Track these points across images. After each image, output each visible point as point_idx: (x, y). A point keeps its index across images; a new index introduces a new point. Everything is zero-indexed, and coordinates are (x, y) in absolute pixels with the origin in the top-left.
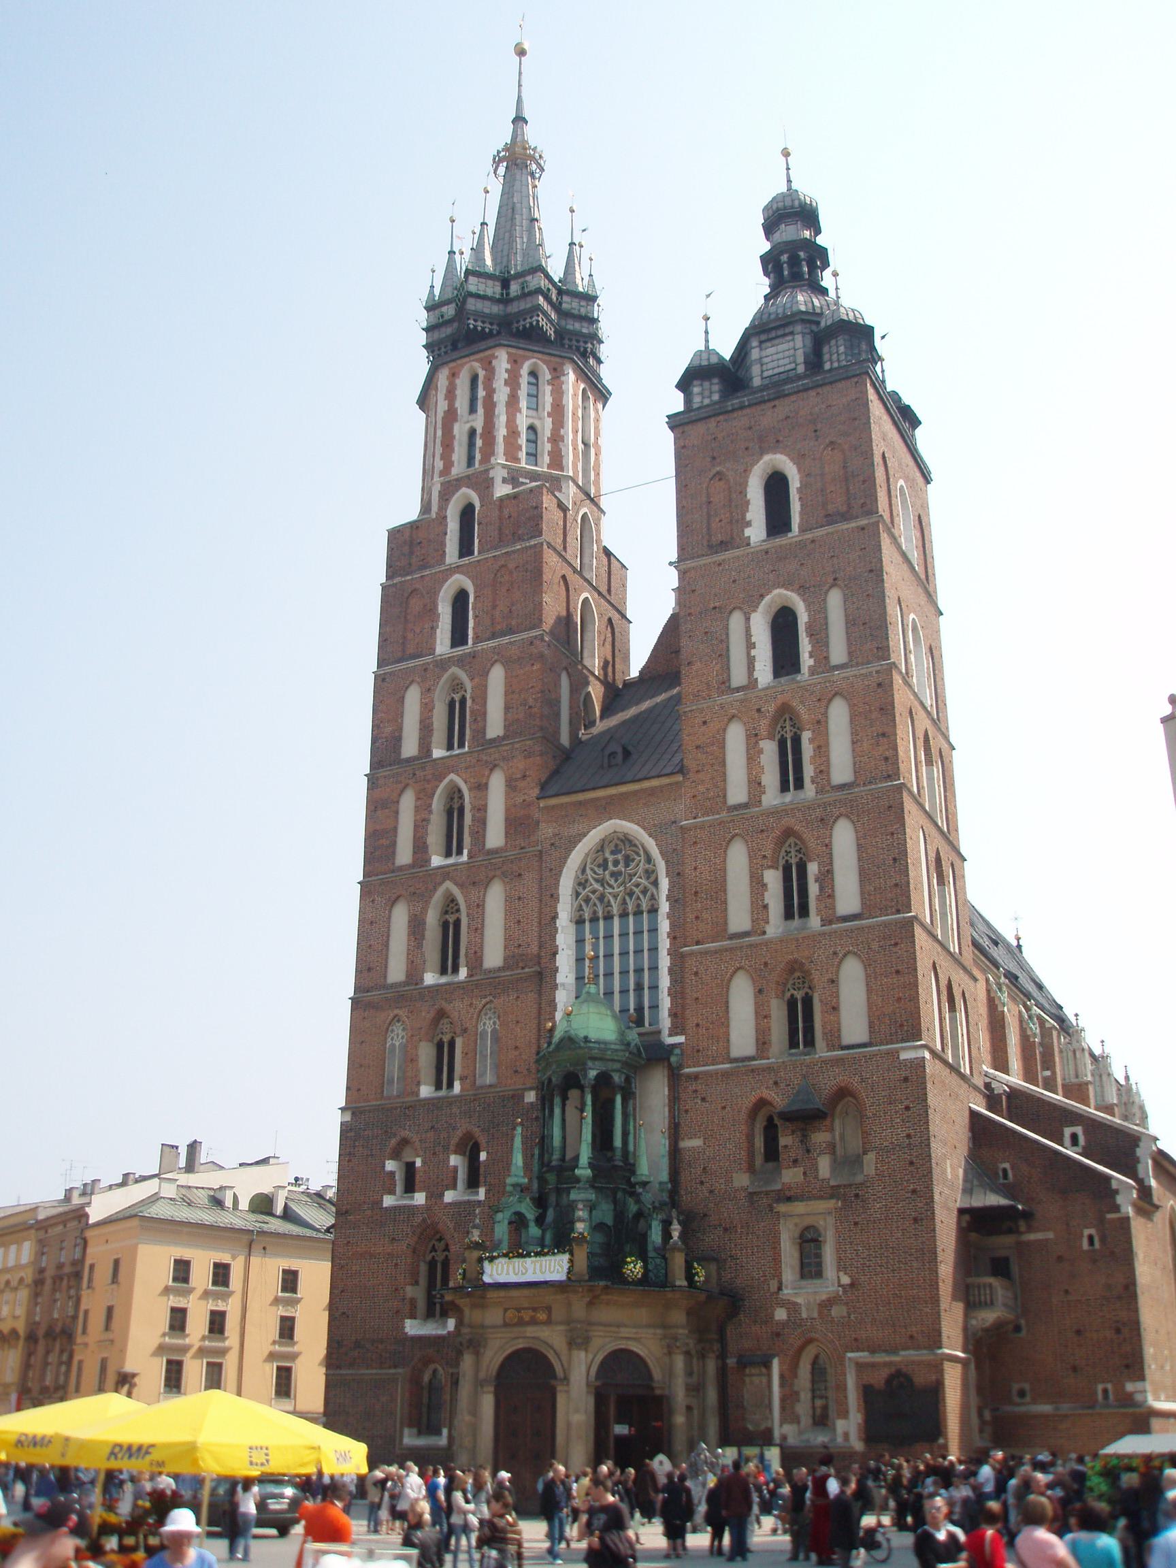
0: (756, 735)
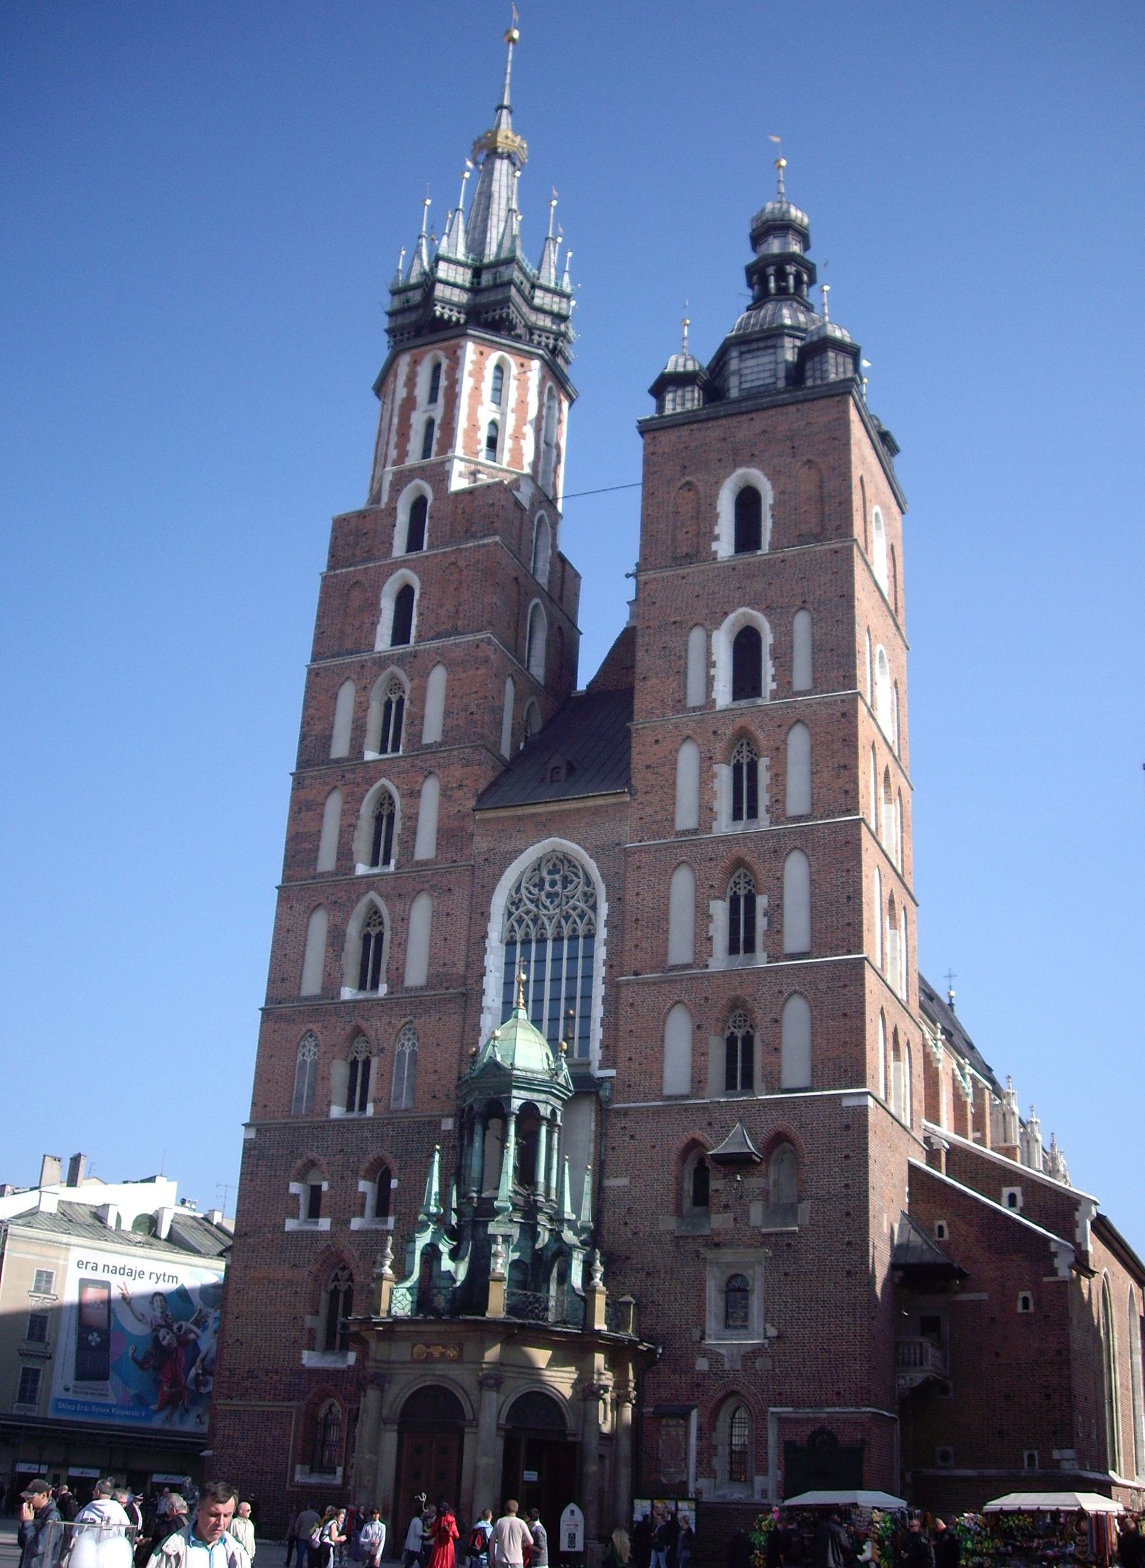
0: (711, 758)
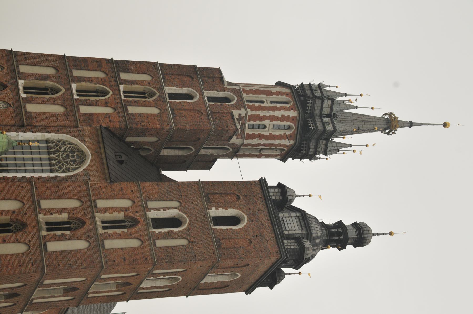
0: (126, 211)
